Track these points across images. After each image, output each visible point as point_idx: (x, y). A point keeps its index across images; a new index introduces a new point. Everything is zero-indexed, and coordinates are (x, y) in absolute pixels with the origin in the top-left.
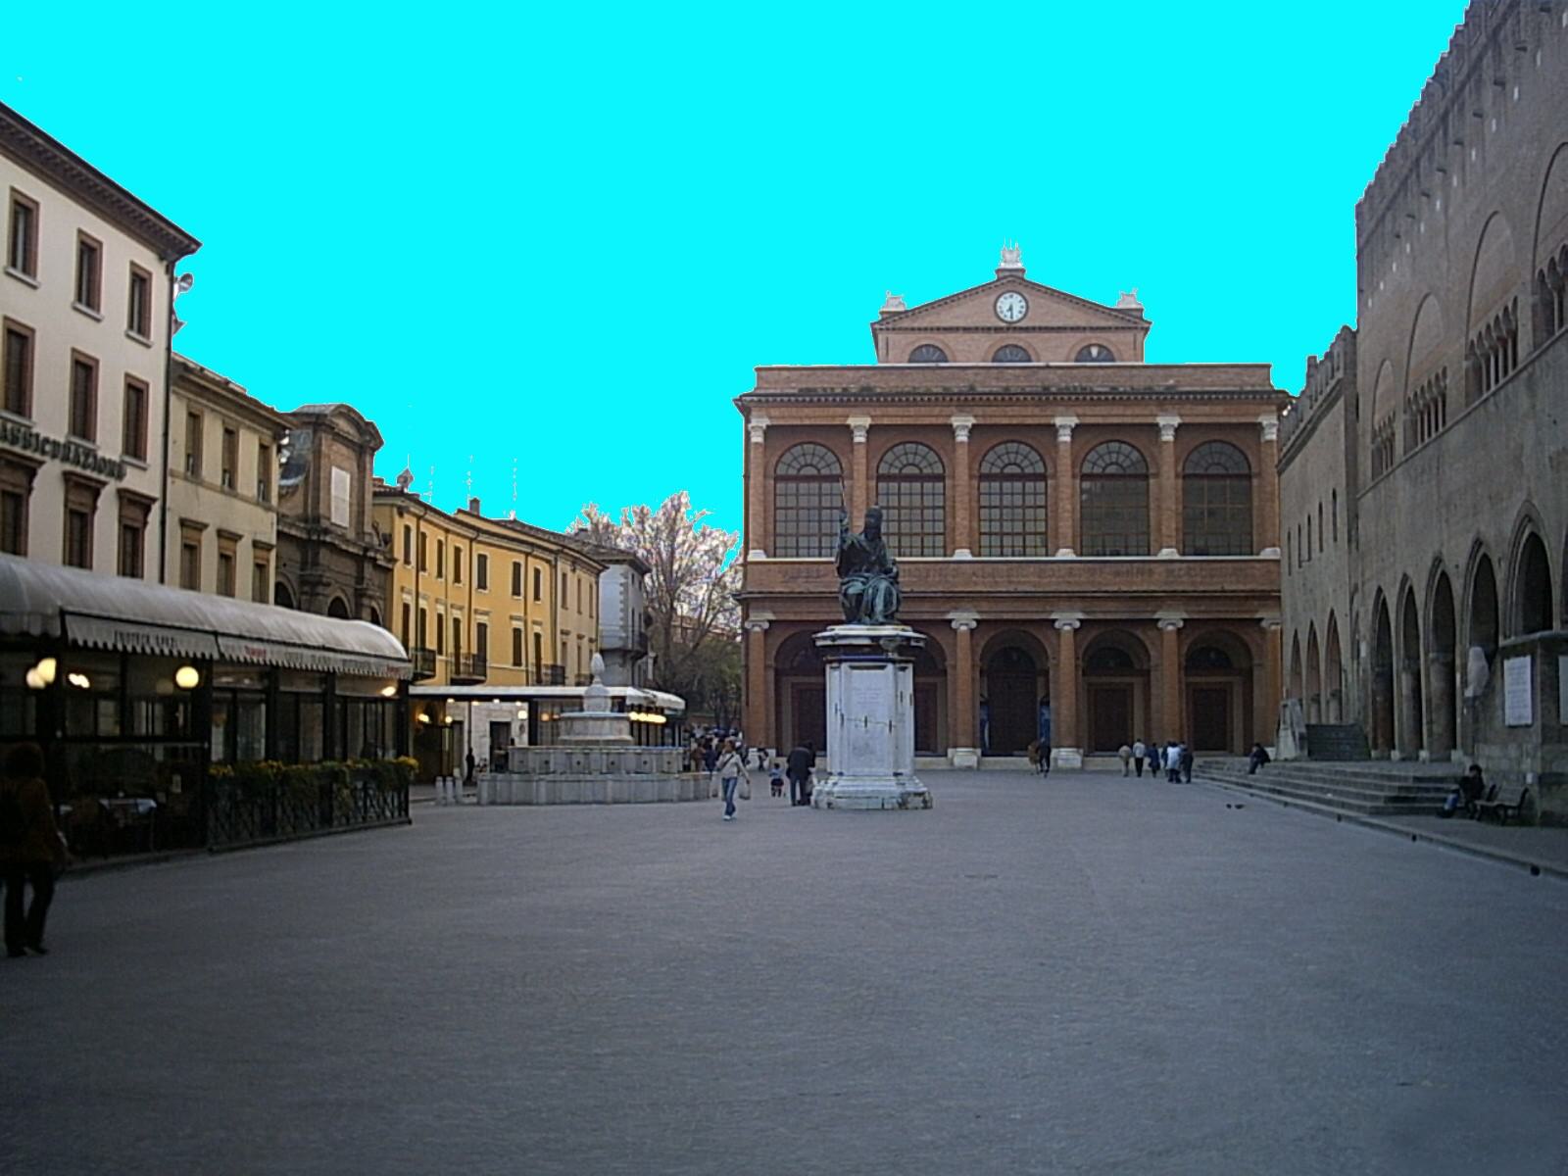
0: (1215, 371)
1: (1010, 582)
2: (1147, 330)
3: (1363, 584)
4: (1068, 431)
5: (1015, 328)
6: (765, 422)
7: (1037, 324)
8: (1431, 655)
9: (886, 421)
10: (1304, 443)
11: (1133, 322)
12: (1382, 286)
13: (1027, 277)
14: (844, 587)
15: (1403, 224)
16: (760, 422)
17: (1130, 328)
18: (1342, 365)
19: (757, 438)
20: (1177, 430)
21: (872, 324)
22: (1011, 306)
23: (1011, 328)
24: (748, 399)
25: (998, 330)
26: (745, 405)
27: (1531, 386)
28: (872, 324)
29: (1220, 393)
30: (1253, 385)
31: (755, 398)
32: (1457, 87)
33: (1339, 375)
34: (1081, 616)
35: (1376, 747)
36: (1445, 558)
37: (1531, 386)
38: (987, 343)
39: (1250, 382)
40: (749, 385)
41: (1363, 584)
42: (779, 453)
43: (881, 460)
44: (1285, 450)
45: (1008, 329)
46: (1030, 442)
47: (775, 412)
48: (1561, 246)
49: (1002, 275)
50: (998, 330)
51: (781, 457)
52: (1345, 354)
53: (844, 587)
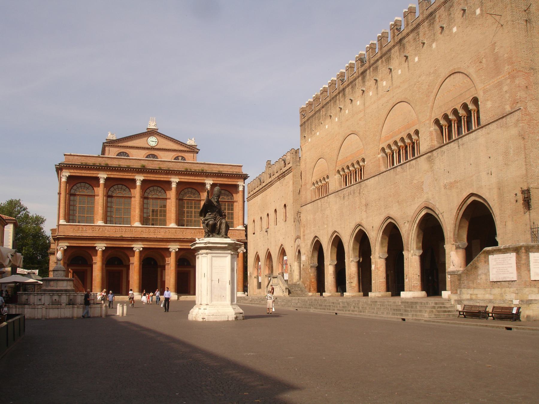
0: (224, 166)
1: (154, 234)
2: (197, 153)
3: (304, 235)
4: (175, 184)
5: (154, 149)
6: (68, 174)
7: (161, 147)
8: (351, 259)
9: (112, 176)
10: (265, 190)
11: (193, 150)
12: (318, 134)
13: (158, 131)
14: (206, 222)
15: (333, 110)
16: (66, 174)
17: (192, 151)
18: (291, 162)
19: (64, 179)
20: (211, 185)
21: (104, 143)
22: (152, 141)
23: (153, 148)
24: (62, 165)
25: (148, 149)
26: (59, 169)
27: (430, 160)
28: (104, 143)
29: (226, 174)
30: (236, 172)
31: (65, 165)
32: (372, 62)
33: (290, 165)
34: (179, 247)
35: (310, 291)
36: (364, 223)
37: (430, 160)
38: (144, 153)
39: (235, 171)
40: (62, 160)
41: (304, 235)
42: (72, 185)
43: (109, 190)
44: (252, 193)
45: (151, 148)
46: (162, 187)
47: (72, 171)
48: (454, 108)
49: (149, 130)
50: (148, 149)
51: (73, 187)
52: (293, 158)
53: (206, 222)
